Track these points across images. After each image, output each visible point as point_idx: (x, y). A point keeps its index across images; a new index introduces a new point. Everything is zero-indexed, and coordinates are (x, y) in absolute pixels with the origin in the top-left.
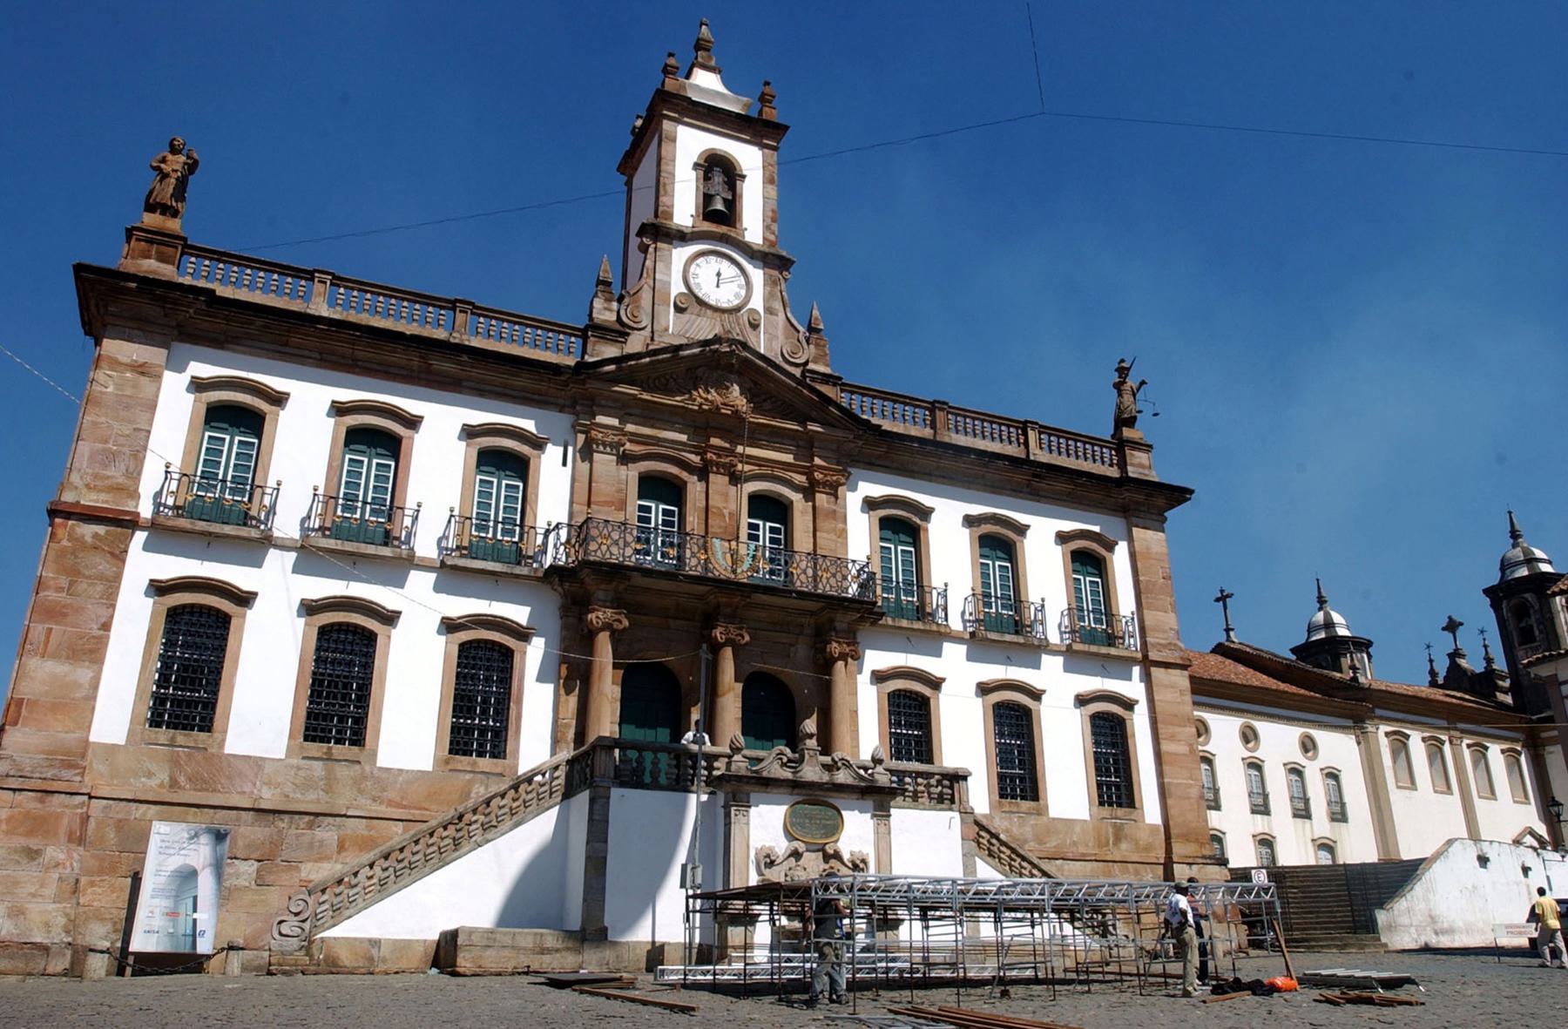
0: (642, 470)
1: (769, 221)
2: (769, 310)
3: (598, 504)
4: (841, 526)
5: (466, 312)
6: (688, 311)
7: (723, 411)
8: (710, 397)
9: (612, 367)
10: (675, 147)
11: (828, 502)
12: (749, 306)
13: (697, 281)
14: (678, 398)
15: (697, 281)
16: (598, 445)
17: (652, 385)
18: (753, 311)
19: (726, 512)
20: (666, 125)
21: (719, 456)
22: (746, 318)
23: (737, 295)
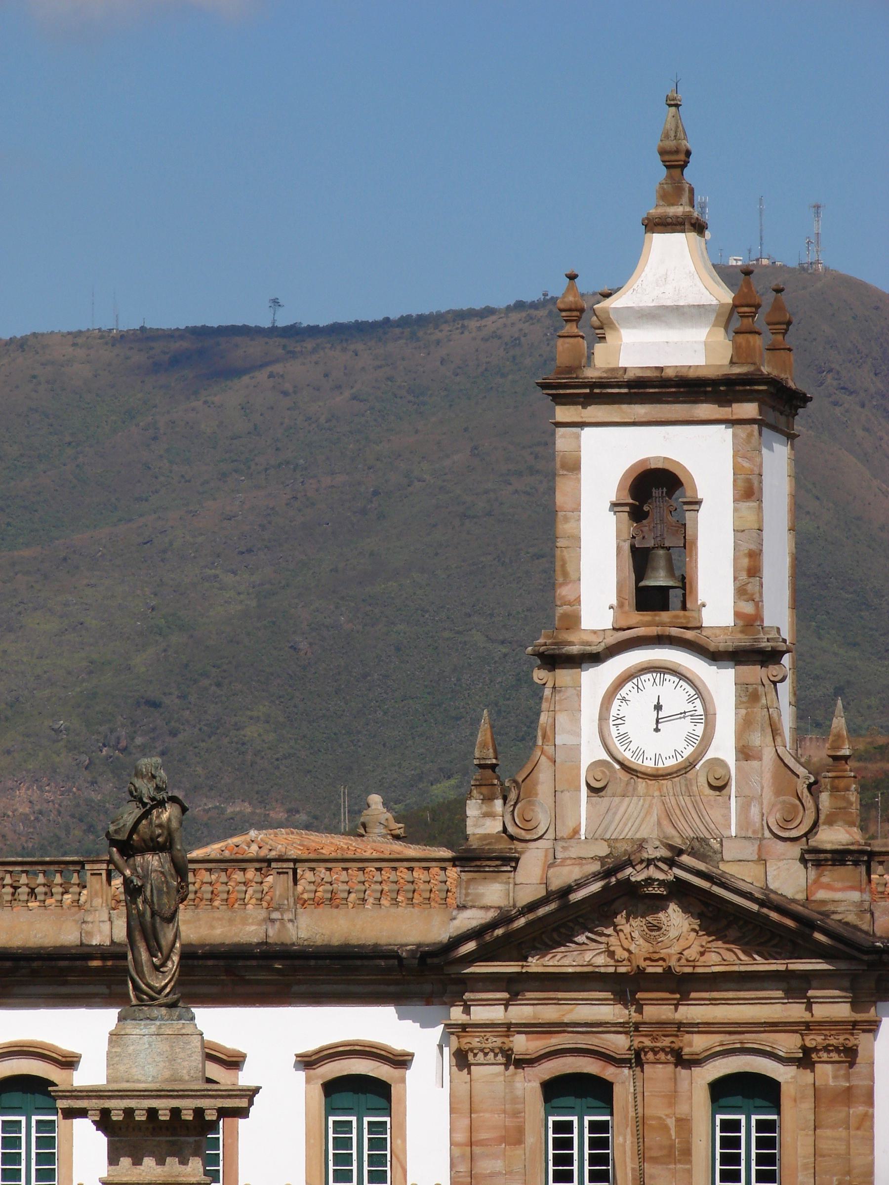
0: (547, 1077)
1: (744, 576)
2: (745, 753)
3: (481, 1143)
4: (861, 1109)
5: (287, 873)
6: (609, 790)
7: (650, 970)
8: (633, 948)
9: (471, 946)
10: (579, 480)
11: (835, 1077)
12: (710, 755)
13: (622, 729)
14: (588, 956)
15: (622, 729)
16: (475, 1055)
17: (550, 943)
18: (718, 762)
19: (671, 1123)
20: (563, 440)
21: (655, 1039)
22: (702, 780)
23: (689, 739)
